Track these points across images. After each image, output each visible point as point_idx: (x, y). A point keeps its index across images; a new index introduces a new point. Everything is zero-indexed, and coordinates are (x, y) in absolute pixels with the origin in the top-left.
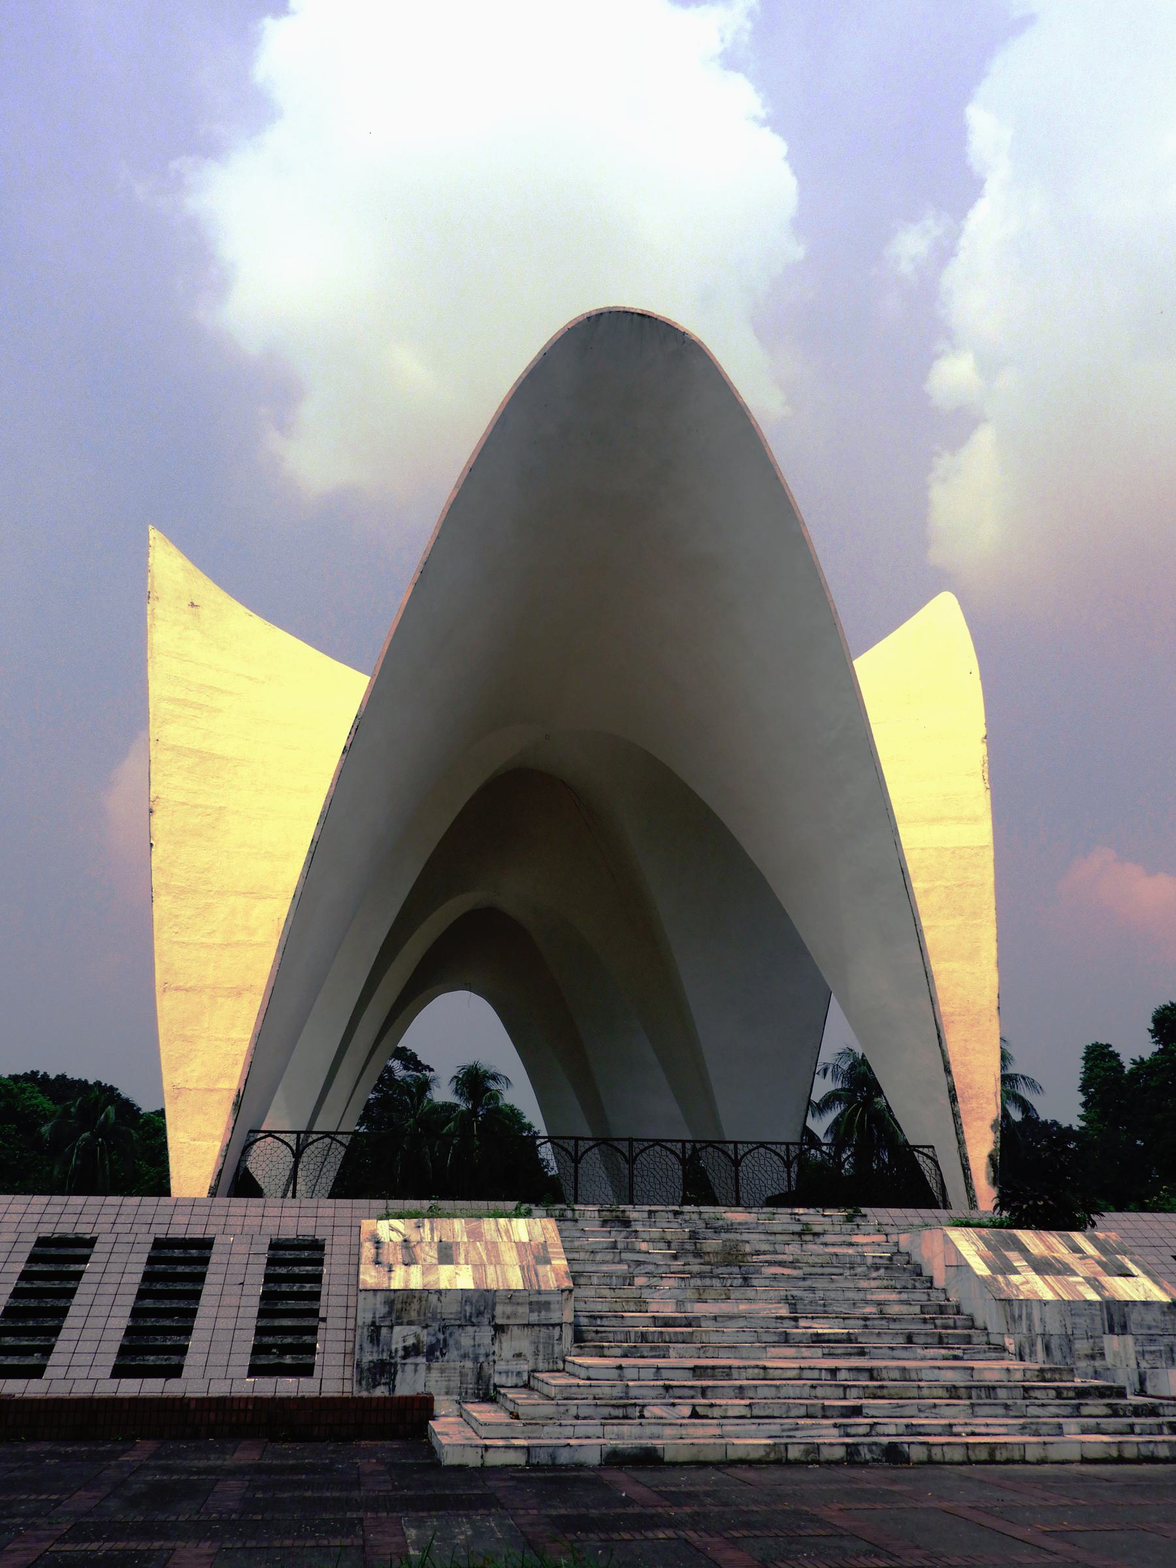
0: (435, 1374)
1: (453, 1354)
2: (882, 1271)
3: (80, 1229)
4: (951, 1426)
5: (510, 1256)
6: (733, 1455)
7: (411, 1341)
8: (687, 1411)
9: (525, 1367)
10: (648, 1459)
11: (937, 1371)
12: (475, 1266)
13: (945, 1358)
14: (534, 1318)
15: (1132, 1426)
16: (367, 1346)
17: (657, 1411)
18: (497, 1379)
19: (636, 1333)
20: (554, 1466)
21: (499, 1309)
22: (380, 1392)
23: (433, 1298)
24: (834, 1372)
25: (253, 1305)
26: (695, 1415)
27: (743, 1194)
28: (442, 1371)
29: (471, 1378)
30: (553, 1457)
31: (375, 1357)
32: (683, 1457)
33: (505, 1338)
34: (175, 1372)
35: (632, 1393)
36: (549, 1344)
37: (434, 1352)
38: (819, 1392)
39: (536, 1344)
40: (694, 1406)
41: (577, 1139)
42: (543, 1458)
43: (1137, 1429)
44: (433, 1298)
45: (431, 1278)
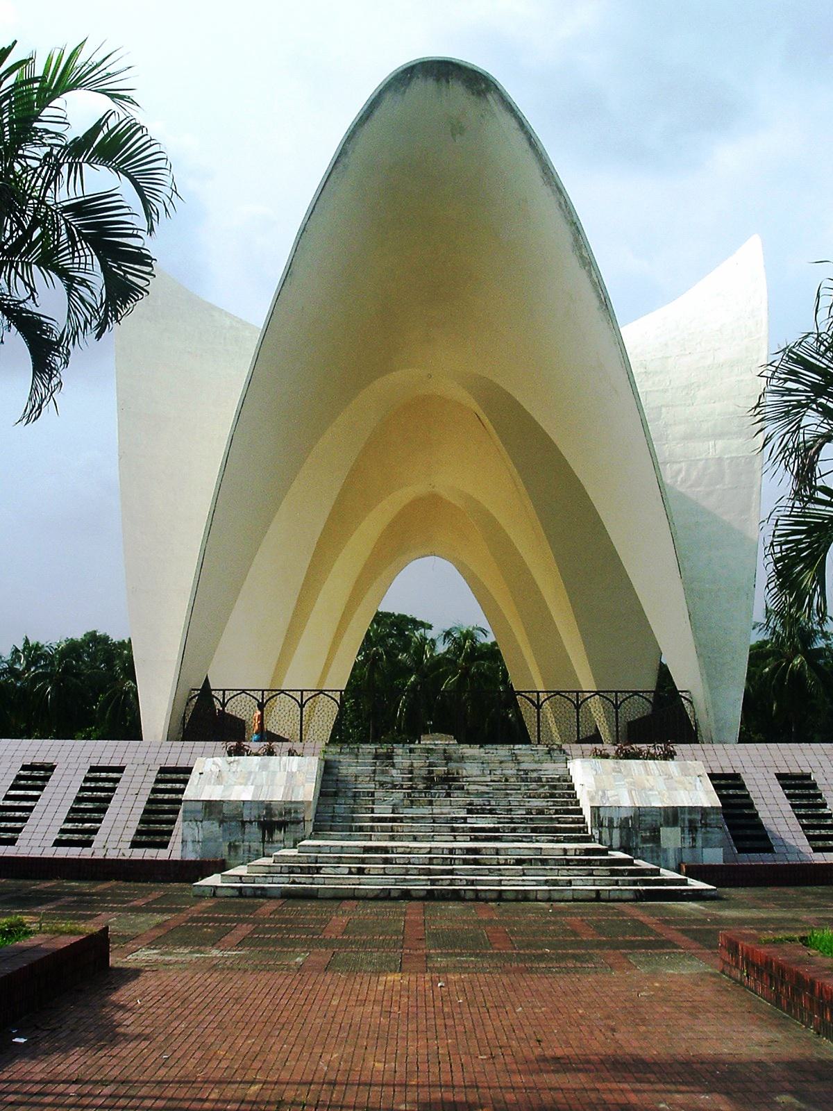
2: (547, 787)
3: (47, 761)
4: (501, 880)
5: (281, 778)
8: (347, 871)
11: (518, 850)
12: (256, 786)
13: (552, 841)
15: (617, 881)
17: (328, 870)
19: (356, 826)
25: (142, 805)
34: (88, 844)
40: (350, 868)
43: (620, 883)
45: (227, 793)
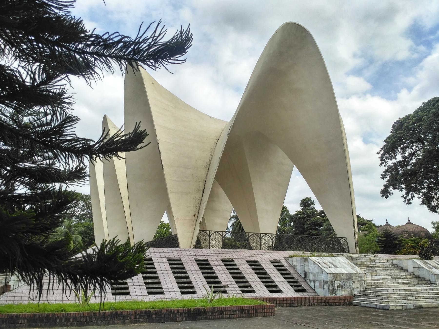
0: (343, 292)
1: (346, 287)
6: (433, 306)
7: (338, 284)
8: (415, 298)
9: (359, 290)
10: (421, 307)
14: (359, 279)
16: (330, 285)
18: (355, 293)
20: (407, 309)
21: (353, 277)
22: (334, 295)
23: (341, 275)
24: (427, 289)
26: (416, 299)
27: (263, 245)
28: (345, 291)
29: (350, 292)
30: (406, 307)
31: (332, 288)
32: (426, 307)
33: (355, 284)
35: (401, 295)
36: (363, 285)
37: (343, 287)
38: (429, 294)
39: (360, 285)
41: (272, 234)
42: (405, 308)
44: (341, 275)
